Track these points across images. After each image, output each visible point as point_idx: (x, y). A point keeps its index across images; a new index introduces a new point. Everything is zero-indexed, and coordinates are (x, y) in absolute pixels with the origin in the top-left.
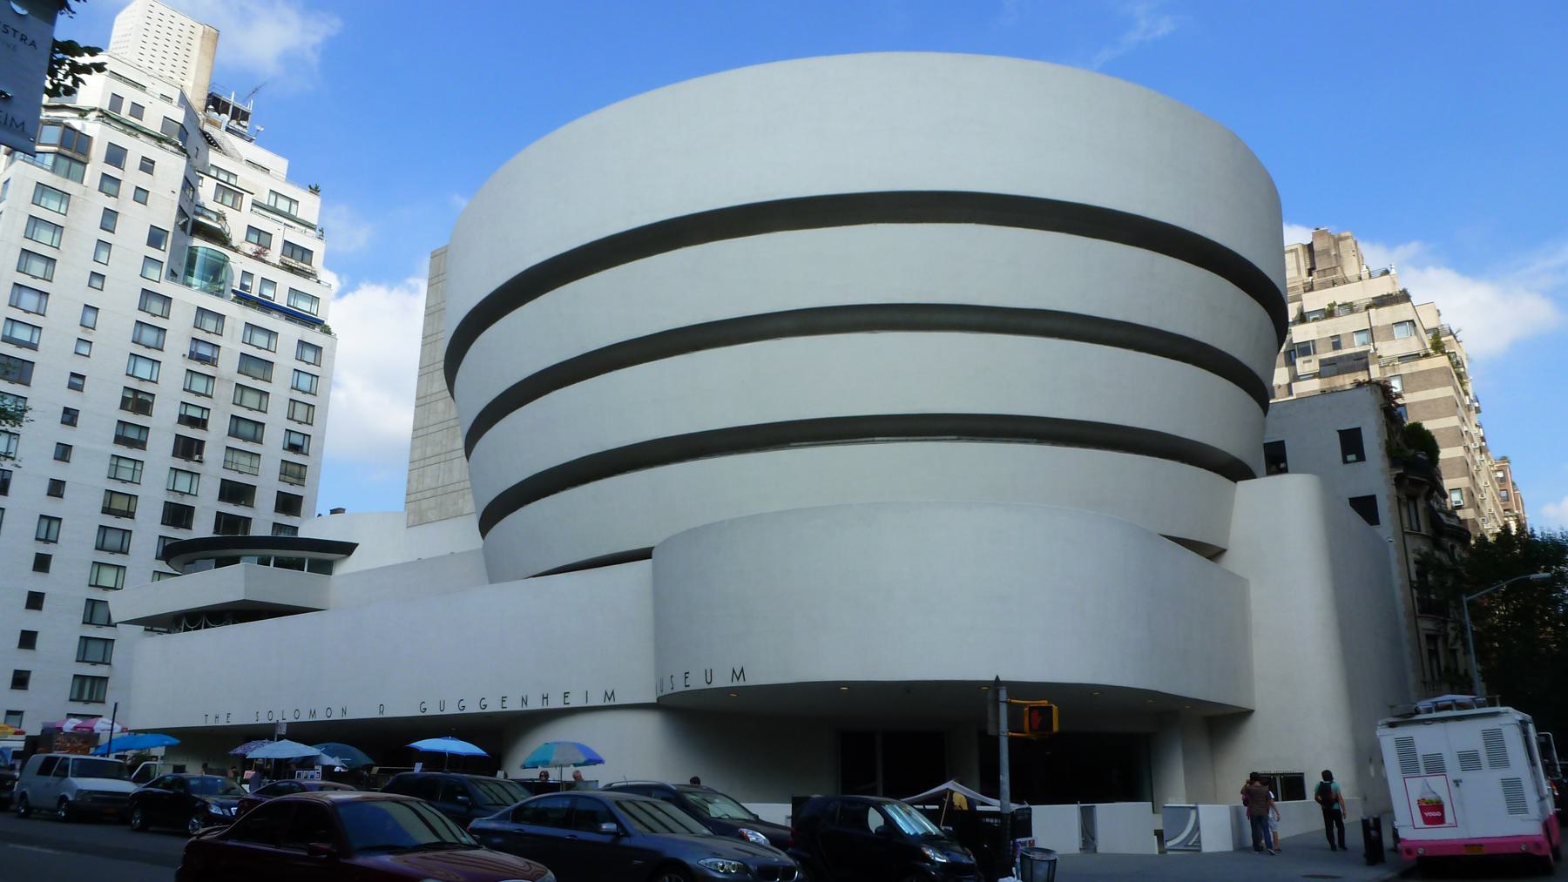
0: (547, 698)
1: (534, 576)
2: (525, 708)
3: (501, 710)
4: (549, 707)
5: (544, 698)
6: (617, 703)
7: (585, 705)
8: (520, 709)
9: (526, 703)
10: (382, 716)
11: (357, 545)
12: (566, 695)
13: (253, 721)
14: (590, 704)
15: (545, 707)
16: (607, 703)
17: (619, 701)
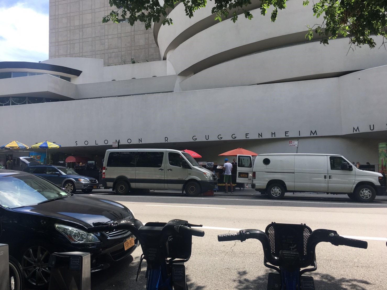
0: (275, 134)
1: (258, 84)
2: (260, 138)
3: (245, 139)
4: (276, 137)
5: (272, 134)
6: (318, 135)
7: (299, 136)
8: (258, 138)
9: (261, 136)
10: (166, 142)
11: (81, 72)
12: (286, 133)
13: (73, 145)
14: (301, 136)
15: (273, 137)
16: (312, 135)
17: (319, 135)
